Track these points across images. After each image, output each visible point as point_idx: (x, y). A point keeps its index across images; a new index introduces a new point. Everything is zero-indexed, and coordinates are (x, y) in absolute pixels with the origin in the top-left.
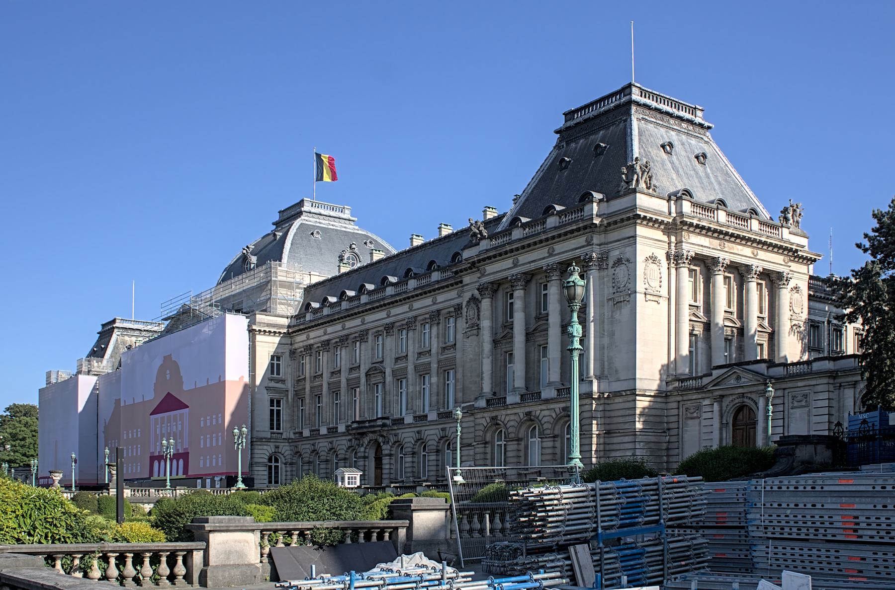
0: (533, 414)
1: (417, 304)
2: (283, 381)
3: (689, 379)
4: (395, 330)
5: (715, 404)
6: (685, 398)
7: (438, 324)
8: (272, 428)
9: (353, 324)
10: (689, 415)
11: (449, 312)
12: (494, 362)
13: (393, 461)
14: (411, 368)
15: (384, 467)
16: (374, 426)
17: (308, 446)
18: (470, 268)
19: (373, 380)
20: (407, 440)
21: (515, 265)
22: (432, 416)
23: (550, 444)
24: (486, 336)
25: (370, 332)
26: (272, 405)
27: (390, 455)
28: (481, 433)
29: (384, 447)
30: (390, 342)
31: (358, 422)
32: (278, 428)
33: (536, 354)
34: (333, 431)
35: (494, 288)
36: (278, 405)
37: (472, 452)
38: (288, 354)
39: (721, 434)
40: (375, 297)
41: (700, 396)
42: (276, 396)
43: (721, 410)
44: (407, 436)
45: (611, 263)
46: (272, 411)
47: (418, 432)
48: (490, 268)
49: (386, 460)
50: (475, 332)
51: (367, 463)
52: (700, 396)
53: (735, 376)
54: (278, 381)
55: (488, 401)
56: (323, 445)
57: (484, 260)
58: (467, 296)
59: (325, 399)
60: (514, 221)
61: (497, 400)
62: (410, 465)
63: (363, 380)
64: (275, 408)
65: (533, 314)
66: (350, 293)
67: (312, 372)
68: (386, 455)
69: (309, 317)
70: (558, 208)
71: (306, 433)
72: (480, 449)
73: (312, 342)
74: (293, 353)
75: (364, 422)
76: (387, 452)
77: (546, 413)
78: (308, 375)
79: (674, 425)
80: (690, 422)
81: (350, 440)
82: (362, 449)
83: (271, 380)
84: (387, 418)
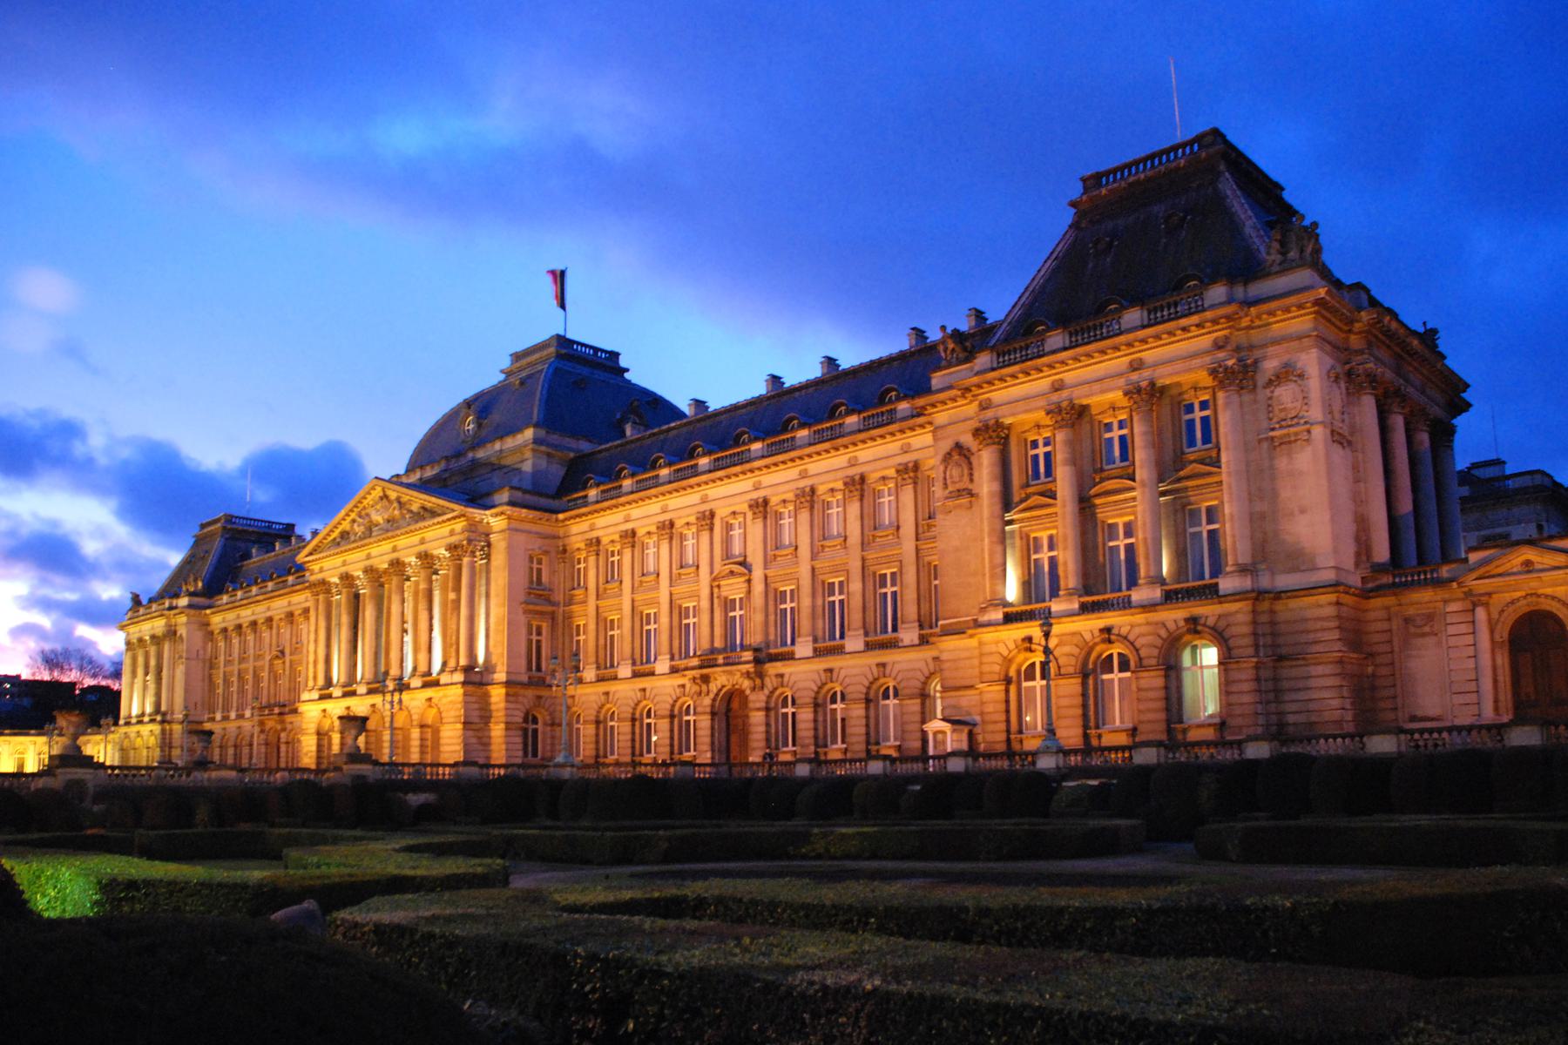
8: (529, 669)
29: (752, 697)
39: (1494, 660)
43: (1489, 620)
64: (534, 638)
76: (758, 705)
80: (1419, 641)
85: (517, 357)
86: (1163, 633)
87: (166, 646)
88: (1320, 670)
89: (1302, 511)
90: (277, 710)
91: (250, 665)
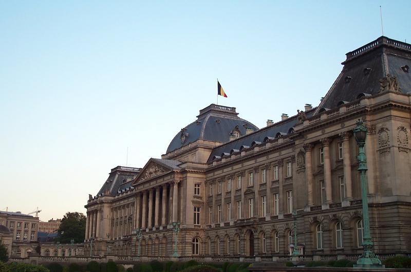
1: (271, 156)
2: (201, 198)
4: (260, 170)
7: (283, 166)
9: (237, 167)
12: (314, 187)
15: (255, 245)
16: (249, 222)
17: (214, 233)
19: (249, 197)
20: (267, 230)
22: (281, 217)
24: (309, 172)
25: (246, 171)
26: (195, 210)
29: (255, 234)
30: (257, 176)
31: (241, 220)
32: (198, 223)
33: (338, 182)
34: (227, 224)
36: (198, 211)
37: (303, 237)
38: (203, 183)
42: (198, 205)
44: (267, 228)
45: (377, 131)
46: (195, 214)
47: (273, 226)
48: (310, 136)
49: (256, 242)
50: (303, 170)
51: (245, 243)
54: (198, 197)
55: (312, 208)
56: (222, 233)
58: (298, 151)
61: (316, 209)
63: (243, 197)
64: (197, 212)
65: (335, 159)
67: (216, 192)
69: (215, 164)
71: (213, 225)
73: (216, 177)
74: (206, 183)
75: (244, 220)
76: (256, 237)
77: (346, 215)
78: (214, 195)
81: (236, 230)
83: (194, 197)
86: (350, 216)
87: (98, 214)
88: (394, 231)
89: (389, 176)
90: (129, 237)
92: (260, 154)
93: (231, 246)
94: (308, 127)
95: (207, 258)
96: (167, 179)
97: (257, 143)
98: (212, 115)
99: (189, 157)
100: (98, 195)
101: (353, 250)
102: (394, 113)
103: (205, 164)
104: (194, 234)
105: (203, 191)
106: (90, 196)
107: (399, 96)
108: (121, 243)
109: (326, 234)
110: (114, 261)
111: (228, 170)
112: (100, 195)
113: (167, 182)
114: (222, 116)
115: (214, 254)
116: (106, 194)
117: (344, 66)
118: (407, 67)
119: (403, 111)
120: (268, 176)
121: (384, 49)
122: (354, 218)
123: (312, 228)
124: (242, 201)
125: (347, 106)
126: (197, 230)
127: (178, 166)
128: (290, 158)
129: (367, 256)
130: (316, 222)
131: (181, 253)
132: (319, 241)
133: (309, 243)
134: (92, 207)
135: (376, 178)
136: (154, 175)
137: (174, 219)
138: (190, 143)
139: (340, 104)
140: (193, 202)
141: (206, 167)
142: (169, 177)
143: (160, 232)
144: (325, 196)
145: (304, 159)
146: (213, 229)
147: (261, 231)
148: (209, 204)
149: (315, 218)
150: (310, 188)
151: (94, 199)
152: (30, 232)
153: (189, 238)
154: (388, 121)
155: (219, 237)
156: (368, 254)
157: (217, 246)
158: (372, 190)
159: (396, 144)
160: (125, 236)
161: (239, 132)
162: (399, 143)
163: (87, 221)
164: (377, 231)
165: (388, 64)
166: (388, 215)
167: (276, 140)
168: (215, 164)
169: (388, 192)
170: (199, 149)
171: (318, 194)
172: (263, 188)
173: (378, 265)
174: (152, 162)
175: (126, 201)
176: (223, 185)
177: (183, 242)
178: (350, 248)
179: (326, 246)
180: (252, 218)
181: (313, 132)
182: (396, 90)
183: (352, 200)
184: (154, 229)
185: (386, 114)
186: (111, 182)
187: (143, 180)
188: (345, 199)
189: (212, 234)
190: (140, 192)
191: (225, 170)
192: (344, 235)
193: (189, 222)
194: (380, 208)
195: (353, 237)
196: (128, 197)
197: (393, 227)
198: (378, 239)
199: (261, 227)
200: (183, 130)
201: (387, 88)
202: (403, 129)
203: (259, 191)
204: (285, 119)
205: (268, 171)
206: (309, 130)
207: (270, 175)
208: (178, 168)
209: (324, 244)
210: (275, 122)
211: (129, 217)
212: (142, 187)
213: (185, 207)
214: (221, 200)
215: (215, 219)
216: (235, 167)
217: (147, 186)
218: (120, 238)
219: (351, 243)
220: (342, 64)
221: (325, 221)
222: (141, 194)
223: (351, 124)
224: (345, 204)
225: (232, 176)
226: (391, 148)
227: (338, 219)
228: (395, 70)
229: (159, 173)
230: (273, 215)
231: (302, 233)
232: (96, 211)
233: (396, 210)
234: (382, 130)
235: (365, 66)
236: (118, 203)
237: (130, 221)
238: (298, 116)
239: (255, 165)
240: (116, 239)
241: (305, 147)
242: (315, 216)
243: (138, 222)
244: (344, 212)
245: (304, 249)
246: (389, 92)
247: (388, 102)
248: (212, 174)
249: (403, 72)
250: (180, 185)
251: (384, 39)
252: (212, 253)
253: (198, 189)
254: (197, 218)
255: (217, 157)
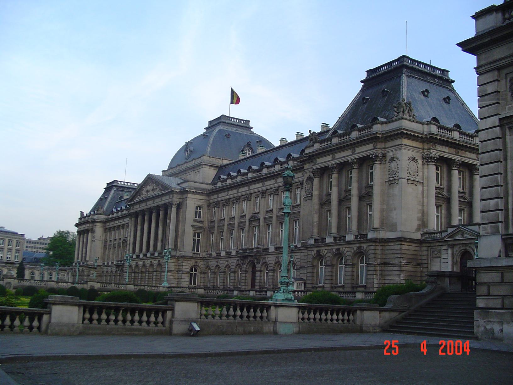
0: (341, 249)
2: (202, 222)
3: (436, 233)
4: (267, 194)
5: (449, 249)
6: (432, 245)
8: (194, 250)
9: (243, 190)
10: (434, 255)
11: (298, 185)
12: (320, 217)
13: (262, 275)
14: (274, 218)
17: (214, 263)
18: (308, 159)
19: (254, 224)
20: (270, 262)
21: (334, 159)
23: (350, 269)
24: (316, 200)
25: (253, 195)
26: (195, 236)
27: (260, 271)
28: (311, 260)
29: (257, 266)
31: (243, 250)
32: (198, 250)
34: (229, 254)
35: (324, 172)
36: (199, 237)
38: (206, 206)
40: (256, 174)
41: (440, 244)
42: (198, 231)
43: (453, 254)
44: (271, 260)
46: (194, 240)
47: (277, 258)
48: (319, 160)
49: (258, 274)
50: (310, 198)
52: (440, 244)
53: (460, 233)
55: (316, 241)
56: (223, 263)
57: (316, 155)
58: (307, 176)
59: (225, 234)
60: (335, 132)
61: (320, 241)
62: (272, 277)
63: (247, 223)
65: (344, 188)
66: (243, 171)
68: (258, 271)
69: (219, 184)
70: (359, 126)
71: (214, 254)
72: (310, 270)
73: (220, 199)
74: (209, 205)
75: (246, 250)
76: (258, 269)
79: (425, 262)
80: (435, 260)
81: (238, 260)
82: (245, 266)
83: (195, 221)
84: (259, 248)
85: (210, 122)
87: (90, 234)
88: (395, 268)
89: (395, 209)
91: (117, 242)
92: (268, 177)
93: (231, 278)
94: (319, 150)
95: (199, 290)
96: (166, 200)
97: (266, 163)
98: (222, 128)
99: (191, 176)
100: (90, 213)
101: (353, 287)
102: (406, 142)
103: (209, 184)
104: (192, 263)
105: (205, 215)
106: (82, 213)
107: (413, 123)
108: (114, 269)
109: (329, 269)
110: (96, 288)
111: (233, 193)
112: (92, 213)
113: (165, 202)
114: (233, 129)
115: (214, 286)
116: (99, 212)
117: (363, 84)
118: (427, 91)
119: (413, 140)
120: (248, 207)
121: (405, 70)
122: (357, 253)
123: (315, 264)
124: (247, 228)
125: (360, 130)
126: (196, 258)
127: (178, 184)
128: (299, 183)
129: (281, 291)
130: (319, 256)
131: (176, 283)
132: (321, 276)
133: (310, 278)
134: (84, 226)
135: (382, 211)
136: (151, 194)
137: (170, 245)
138: (194, 159)
139: (354, 127)
140: (193, 227)
141: (210, 187)
142: (167, 197)
143: (155, 258)
144: (330, 229)
145: (313, 186)
146: (214, 258)
147: (264, 263)
148: (211, 229)
149: (319, 251)
150: (316, 219)
151: (85, 217)
152: (14, 251)
153: (186, 266)
154: (398, 150)
155: (219, 268)
156: (282, 290)
157: (217, 277)
158: (376, 223)
159: (405, 176)
160: (118, 261)
161: (251, 148)
162: (408, 175)
163: (77, 242)
164: (378, 268)
165: (408, 88)
166: (392, 252)
167: (286, 162)
168: (219, 184)
169: (393, 227)
170: (204, 166)
171: (323, 226)
172: (269, 215)
173: (290, 300)
174: (150, 179)
175: (121, 221)
176: (226, 209)
177: (179, 271)
178: (350, 285)
179: (327, 281)
180: (255, 248)
181: (323, 156)
182: (410, 116)
183: (357, 233)
184: (149, 255)
185: (398, 142)
186: (106, 198)
187: (140, 198)
188: (350, 231)
189: (213, 264)
190: (136, 212)
191: (230, 193)
192: (345, 271)
193: (187, 248)
194: (383, 244)
195: (355, 273)
196: (123, 217)
197: (394, 264)
198: (378, 277)
199: (264, 259)
200: (188, 144)
201: (401, 114)
202: (414, 159)
203: (265, 219)
204: (299, 138)
205: (276, 196)
206: (319, 154)
207: (277, 201)
208: (178, 187)
209: (325, 280)
210: (289, 140)
211: (124, 240)
212: (138, 206)
213: (184, 231)
214: (224, 225)
215: (217, 247)
216: (241, 190)
217: (143, 206)
218: (112, 263)
219: (352, 279)
220: (362, 82)
221: (328, 255)
222: (136, 215)
223: (363, 151)
224: (350, 237)
225: (238, 200)
226: (400, 180)
227: (341, 254)
228: (414, 94)
229: (157, 192)
230: (277, 246)
231: (304, 267)
232: (86, 232)
233: (398, 247)
234: (392, 159)
235: (384, 86)
236: (112, 223)
237: (125, 244)
238: (309, 136)
239: (263, 188)
240: (108, 263)
241: (314, 172)
242: (318, 249)
243: (131, 246)
244: (348, 246)
245: (305, 284)
246: (402, 119)
247: (399, 130)
248: (215, 196)
249: (422, 96)
250: (179, 206)
251: (405, 59)
252: (212, 284)
253: (200, 212)
254: (196, 245)
255: (222, 177)
